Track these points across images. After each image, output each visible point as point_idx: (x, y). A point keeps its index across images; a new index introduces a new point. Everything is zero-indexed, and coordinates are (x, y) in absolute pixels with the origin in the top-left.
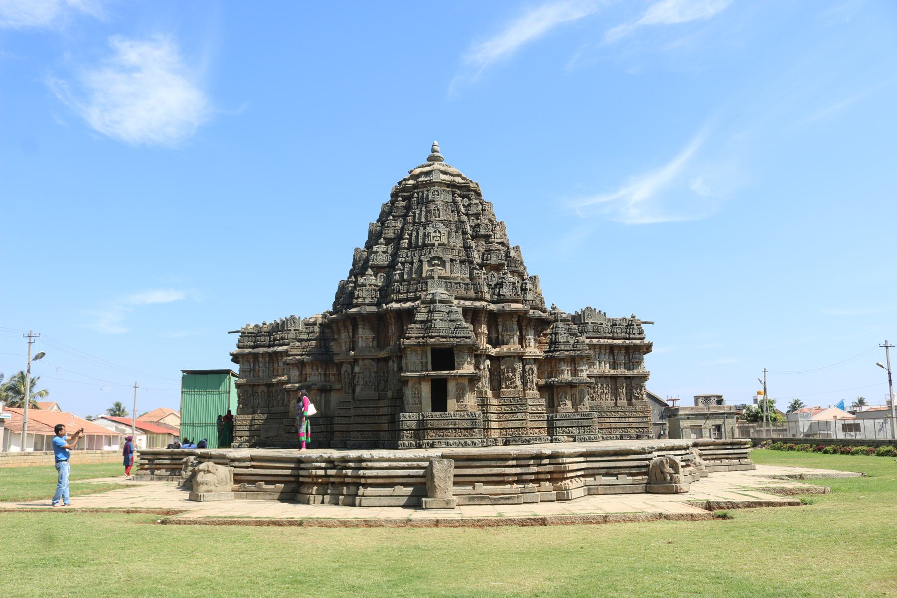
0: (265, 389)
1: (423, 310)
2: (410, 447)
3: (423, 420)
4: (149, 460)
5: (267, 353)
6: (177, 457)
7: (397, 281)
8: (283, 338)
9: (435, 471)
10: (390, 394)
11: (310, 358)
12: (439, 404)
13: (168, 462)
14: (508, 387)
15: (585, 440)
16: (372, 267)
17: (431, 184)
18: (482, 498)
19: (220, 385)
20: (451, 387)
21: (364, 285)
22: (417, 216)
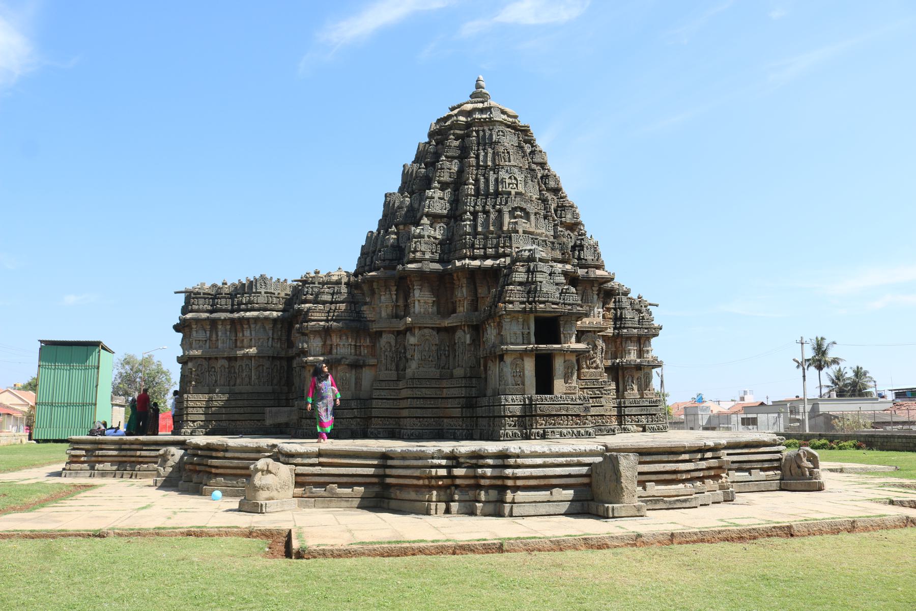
0: (225, 363)
1: (521, 269)
2: (514, 438)
3: (531, 404)
4: (87, 450)
7: (469, 234)
8: (250, 302)
9: (621, 468)
10: (459, 372)
11: (340, 325)
12: (545, 385)
13: (115, 453)
15: (653, 430)
16: (428, 215)
17: (491, 122)
18: (656, 502)
20: (559, 365)
21: (420, 236)
22: (481, 158)
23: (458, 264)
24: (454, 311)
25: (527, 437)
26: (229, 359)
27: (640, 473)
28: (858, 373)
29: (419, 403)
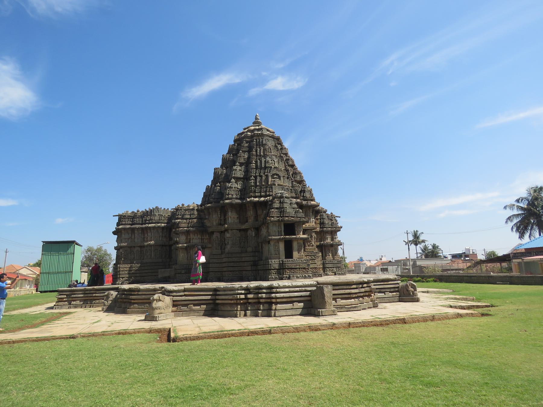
0: (139, 249)
2: (275, 279)
3: (283, 263)
4: (67, 295)
5: (141, 228)
6: (88, 292)
7: (253, 186)
9: (325, 292)
10: (250, 249)
11: (194, 229)
12: (289, 254)
14: (309, 246)
15: (339, 274)
16: (234, 178)
17: (262, 135)
18: (342, 308)
19: (68, 249)
20: (295, 245)
21: (231, 187)
22: (258, 151)
23: (248, 200)
24: (247, 222)
25: (281, 279)
26: (141, 247)
27: (333, 295)
28: (434, 246)
29: (232, 264)
